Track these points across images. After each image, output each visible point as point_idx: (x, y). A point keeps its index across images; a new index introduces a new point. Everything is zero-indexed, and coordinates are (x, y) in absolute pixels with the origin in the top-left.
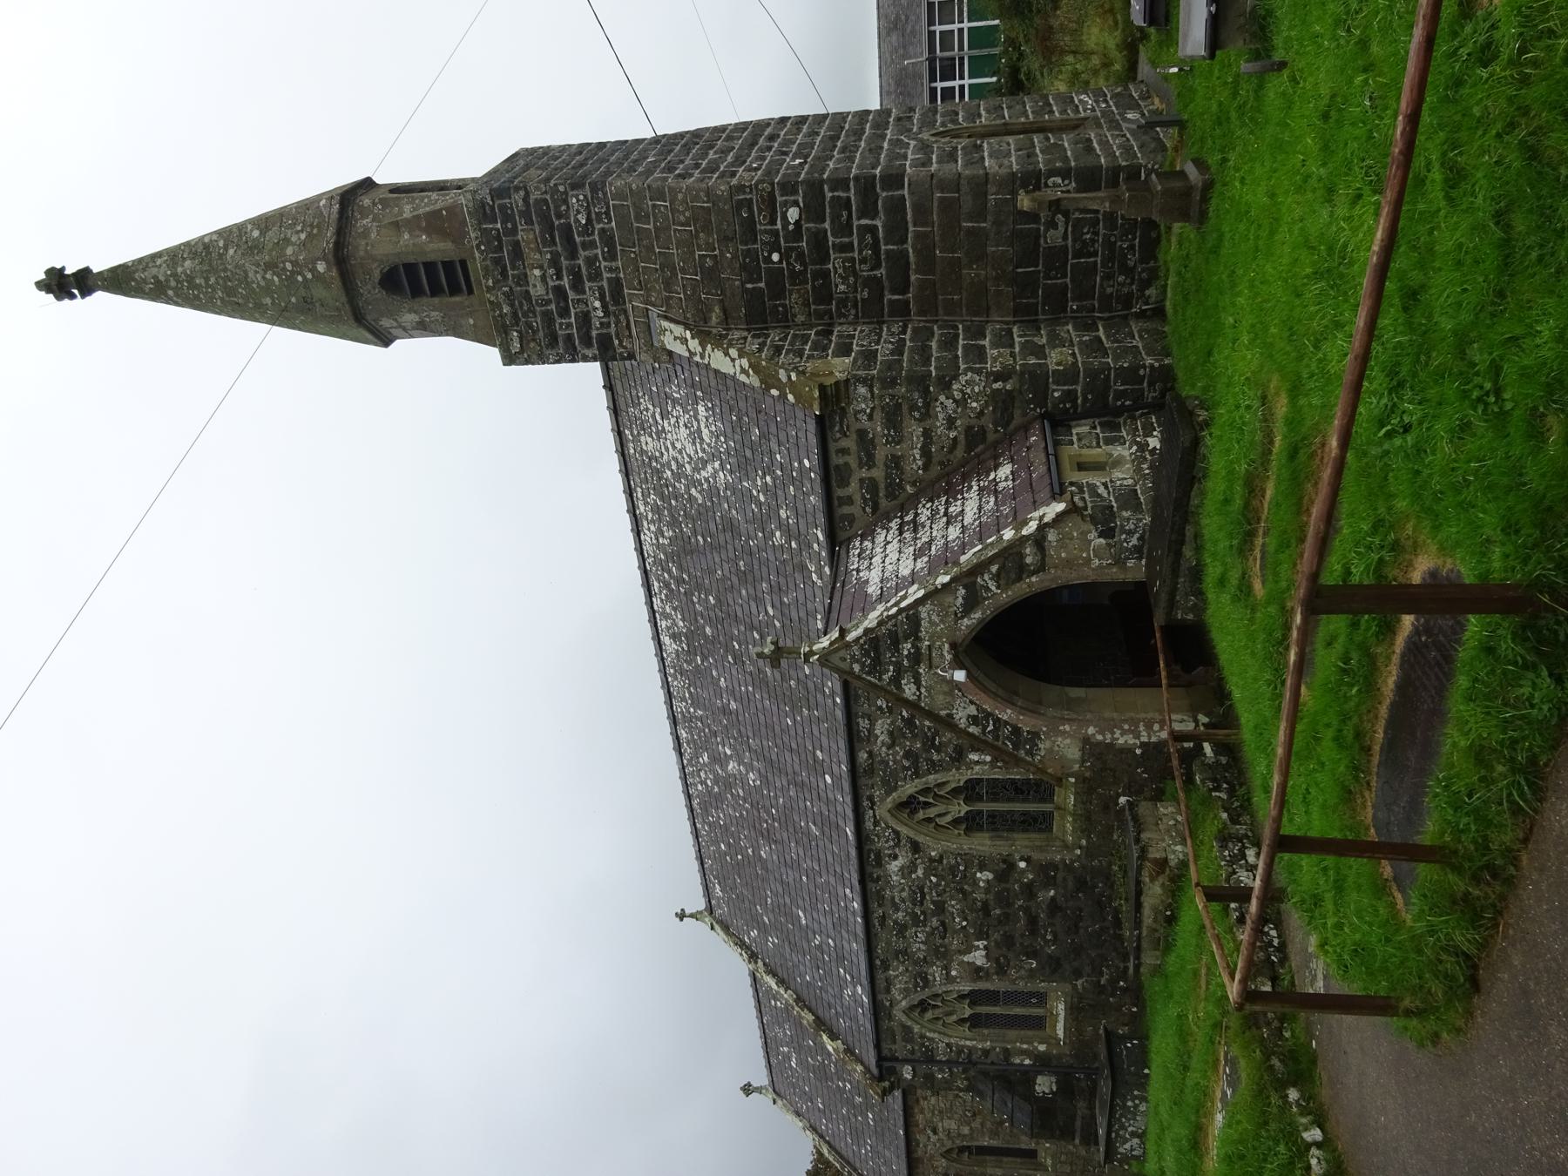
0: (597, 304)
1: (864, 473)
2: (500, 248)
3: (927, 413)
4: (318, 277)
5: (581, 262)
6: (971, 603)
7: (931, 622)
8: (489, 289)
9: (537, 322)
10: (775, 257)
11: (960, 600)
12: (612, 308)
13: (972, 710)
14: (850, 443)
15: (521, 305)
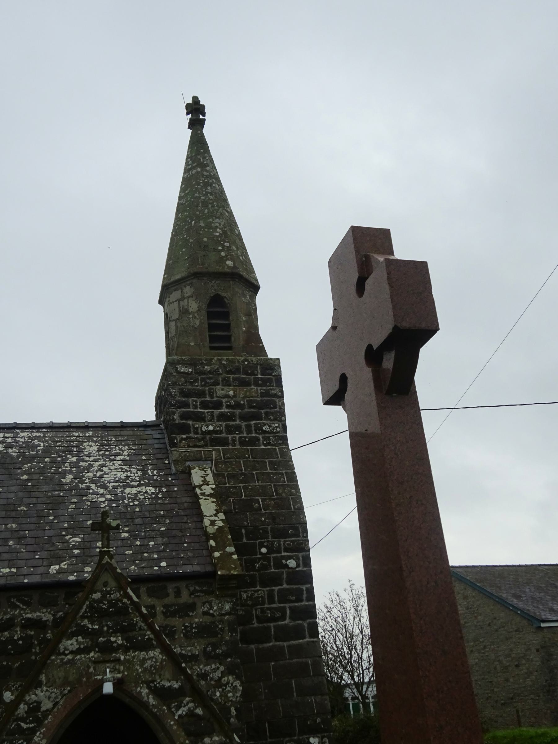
0: (211, 428)
1: (159, 609)
2: (246, 373)
3: (209, 657)
4: (223, 260)
5: (238, 422)
6: (165, 695)
7: (144, 660)
8: (220, 360)
9: (198, 386)
10: (264, 550)
11: (167, 684)
12: (208, 437)
13: (47, 705)
14: (185, 597)
15: (210, 378)
